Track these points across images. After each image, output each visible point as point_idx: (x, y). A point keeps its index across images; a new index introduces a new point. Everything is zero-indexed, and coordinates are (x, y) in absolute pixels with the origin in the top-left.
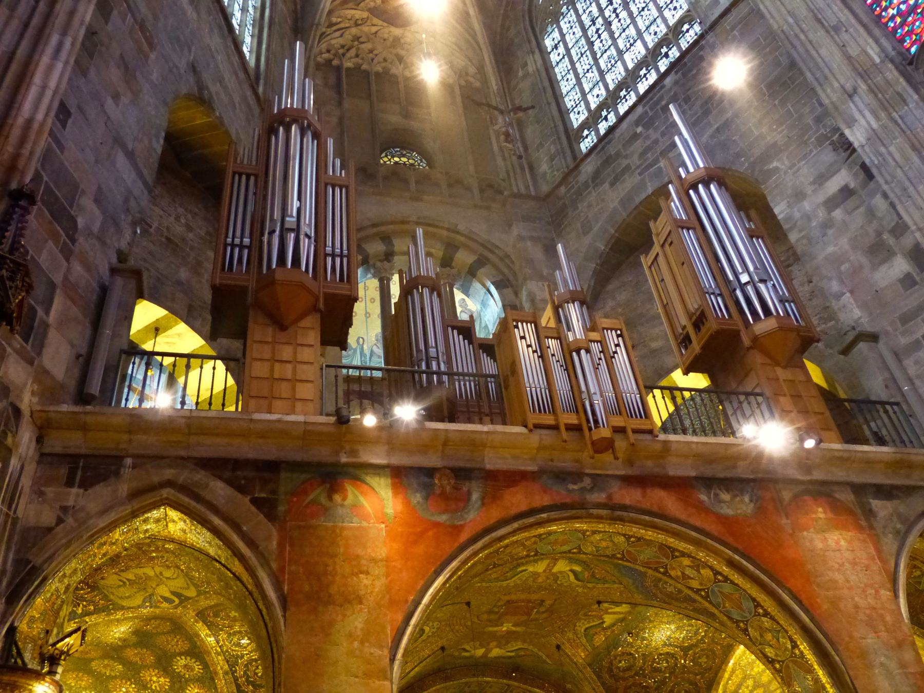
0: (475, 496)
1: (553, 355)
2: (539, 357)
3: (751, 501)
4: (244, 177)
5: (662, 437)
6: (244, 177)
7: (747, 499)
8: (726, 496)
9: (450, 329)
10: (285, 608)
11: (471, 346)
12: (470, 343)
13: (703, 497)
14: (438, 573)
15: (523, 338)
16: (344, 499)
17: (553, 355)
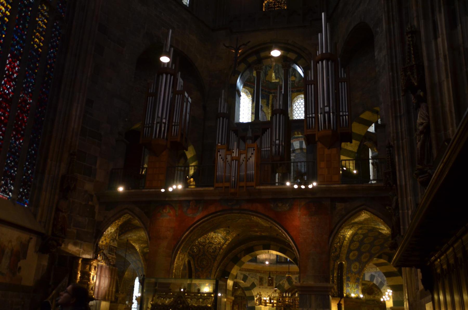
0: (201, 208)
1: (228, 161)
2: (227, 159)
3: (289, 206)
4: (151, 97)
5: (258, 187)
6: (151, 97)
7: (287, 205)
8: (280, 205)
9: (231, 131)
10: (150, 240)
11: (237, 138)
12: (237, 136)
13: (272, 205)
14: (187, 230)
15: (220, 155)
16: (166, 211)
17: (228, 161)
